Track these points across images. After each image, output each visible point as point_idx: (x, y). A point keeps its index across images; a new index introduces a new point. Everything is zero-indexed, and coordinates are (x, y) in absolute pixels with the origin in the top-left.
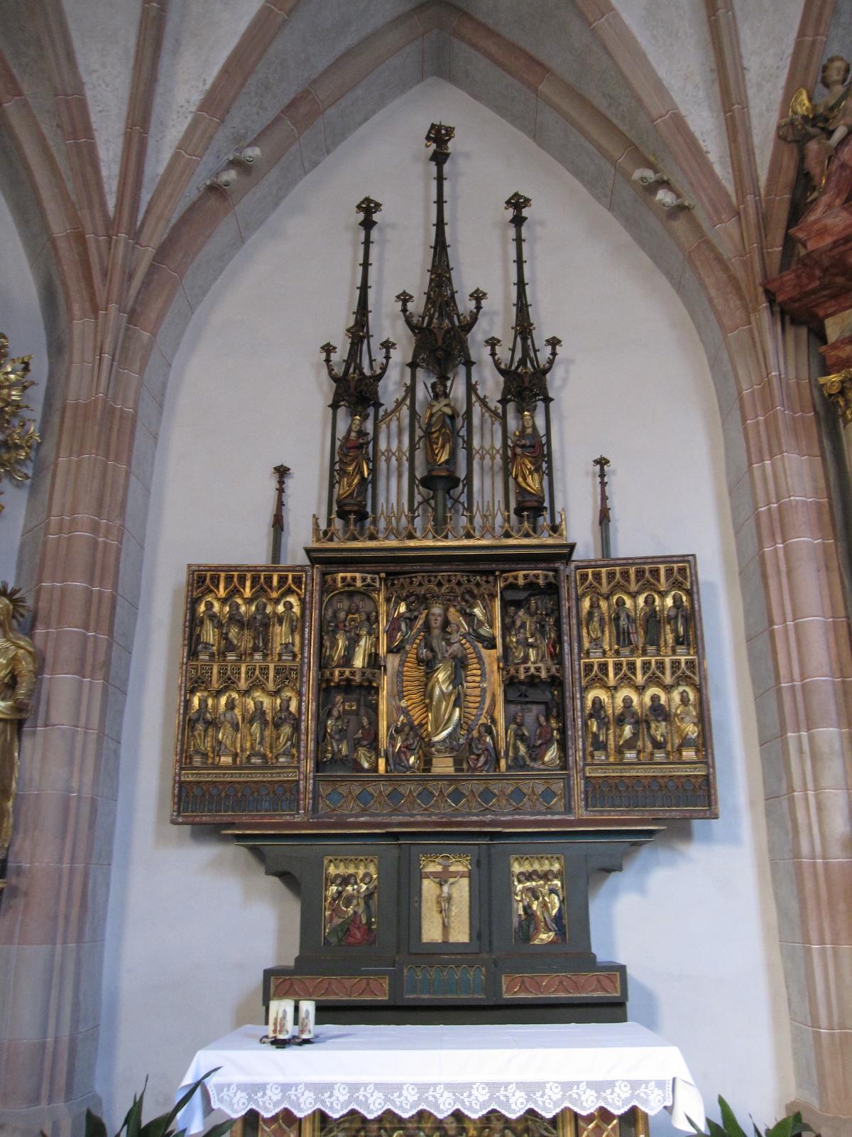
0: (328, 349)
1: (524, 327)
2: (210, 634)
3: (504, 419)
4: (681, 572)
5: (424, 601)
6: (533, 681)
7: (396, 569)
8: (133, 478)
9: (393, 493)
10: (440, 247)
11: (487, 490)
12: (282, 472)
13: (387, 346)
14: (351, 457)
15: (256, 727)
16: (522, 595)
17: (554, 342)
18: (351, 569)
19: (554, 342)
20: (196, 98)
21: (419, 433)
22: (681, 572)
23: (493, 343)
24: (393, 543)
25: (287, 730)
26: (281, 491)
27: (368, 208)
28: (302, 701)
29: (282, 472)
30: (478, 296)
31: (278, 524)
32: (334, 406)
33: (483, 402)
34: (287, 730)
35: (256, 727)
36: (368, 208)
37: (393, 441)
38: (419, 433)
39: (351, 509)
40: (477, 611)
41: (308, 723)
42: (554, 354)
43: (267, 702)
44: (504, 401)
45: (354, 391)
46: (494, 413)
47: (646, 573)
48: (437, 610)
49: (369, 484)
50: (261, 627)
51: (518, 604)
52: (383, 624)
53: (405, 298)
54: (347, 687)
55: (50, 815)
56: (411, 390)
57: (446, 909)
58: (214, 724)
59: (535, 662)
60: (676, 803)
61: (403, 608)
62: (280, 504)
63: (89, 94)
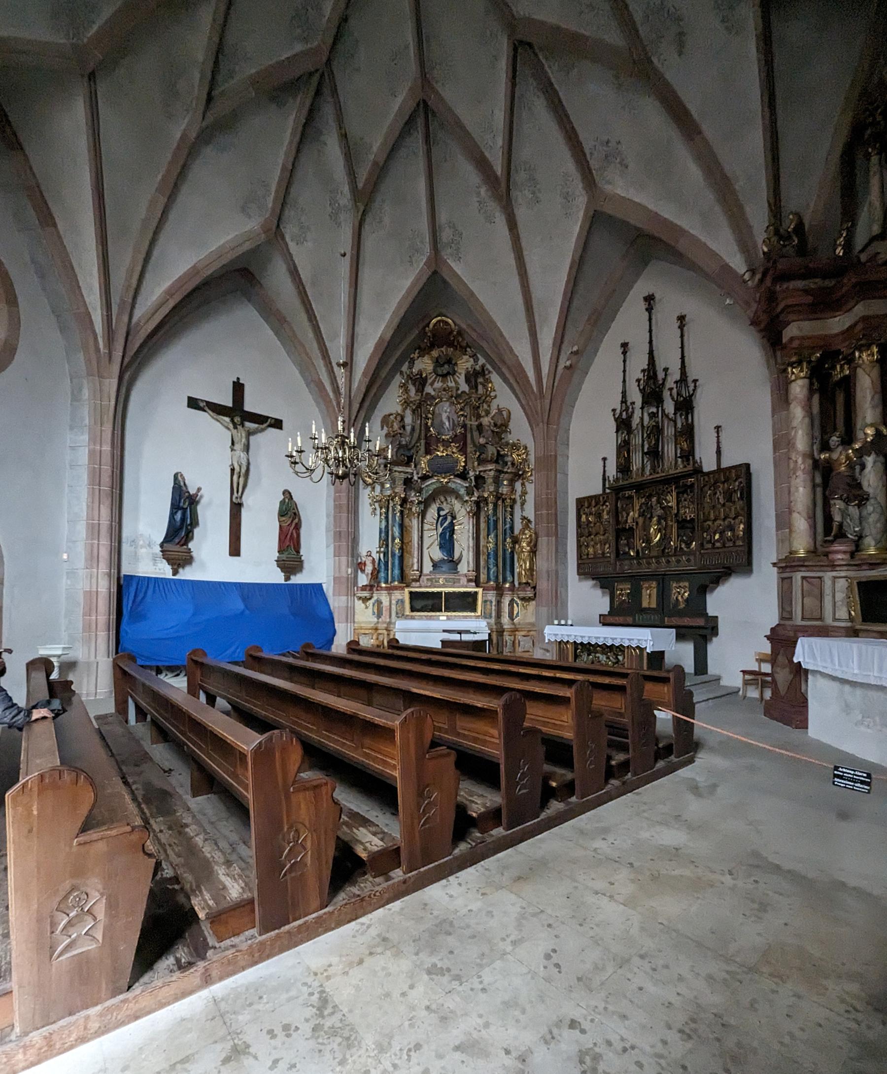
0: (614, 410)
1: (683, 379)
2: (584, 518)
3: (675, 422)
4: (744, 471)
5: (650, 497)
6: (685, 521)
7: (639, 487)
8: (558, 475)
9: (637, 460)
10: (651, 353)
11: (670, 450)
12: (604, 459)
13: (633, 403)
14: (624, 448)
15: (599, 546)
16: (681, 490)
17: (695, 381)
18: (622, 490)
19: (695, 381)
20: (551, 342)
21: (645, 435)
22: (744, 471)
23: (671, 389)
24: (633, 480)
25: (607, 546)
26: (604, 467)
27: (625, 345)
28: (611, 537)
29: (604, 459)
30: (666, 370)
31: (604, 480)
32: (617, 432)
33: (667, 416)
34: (607, 546)
35: (599, 546)
36: (625, 345)
37: (637, 440)
38: (645, 435)
39: (624, 468)
40: (669, 498)
41: (613, 543)
42: (695, 386)
43: (602, 537)
44: (675, 414)
45: (623, 424)
46: (670, 420)
47: (723, 474)
48: (654, 499)
49: (628, 460)
50: (599, 516)
51: (683, 493)
52: (638, 508)
53: (638, 381)
54: (624, 530)
55: (545, 576)
56: (642, 419)
57: (649, 597)
58: (587, 546)
59: (688, 513)
60: (741, 562)
61: (643, 500)
62: (604, 471)
63: (520, 358)
